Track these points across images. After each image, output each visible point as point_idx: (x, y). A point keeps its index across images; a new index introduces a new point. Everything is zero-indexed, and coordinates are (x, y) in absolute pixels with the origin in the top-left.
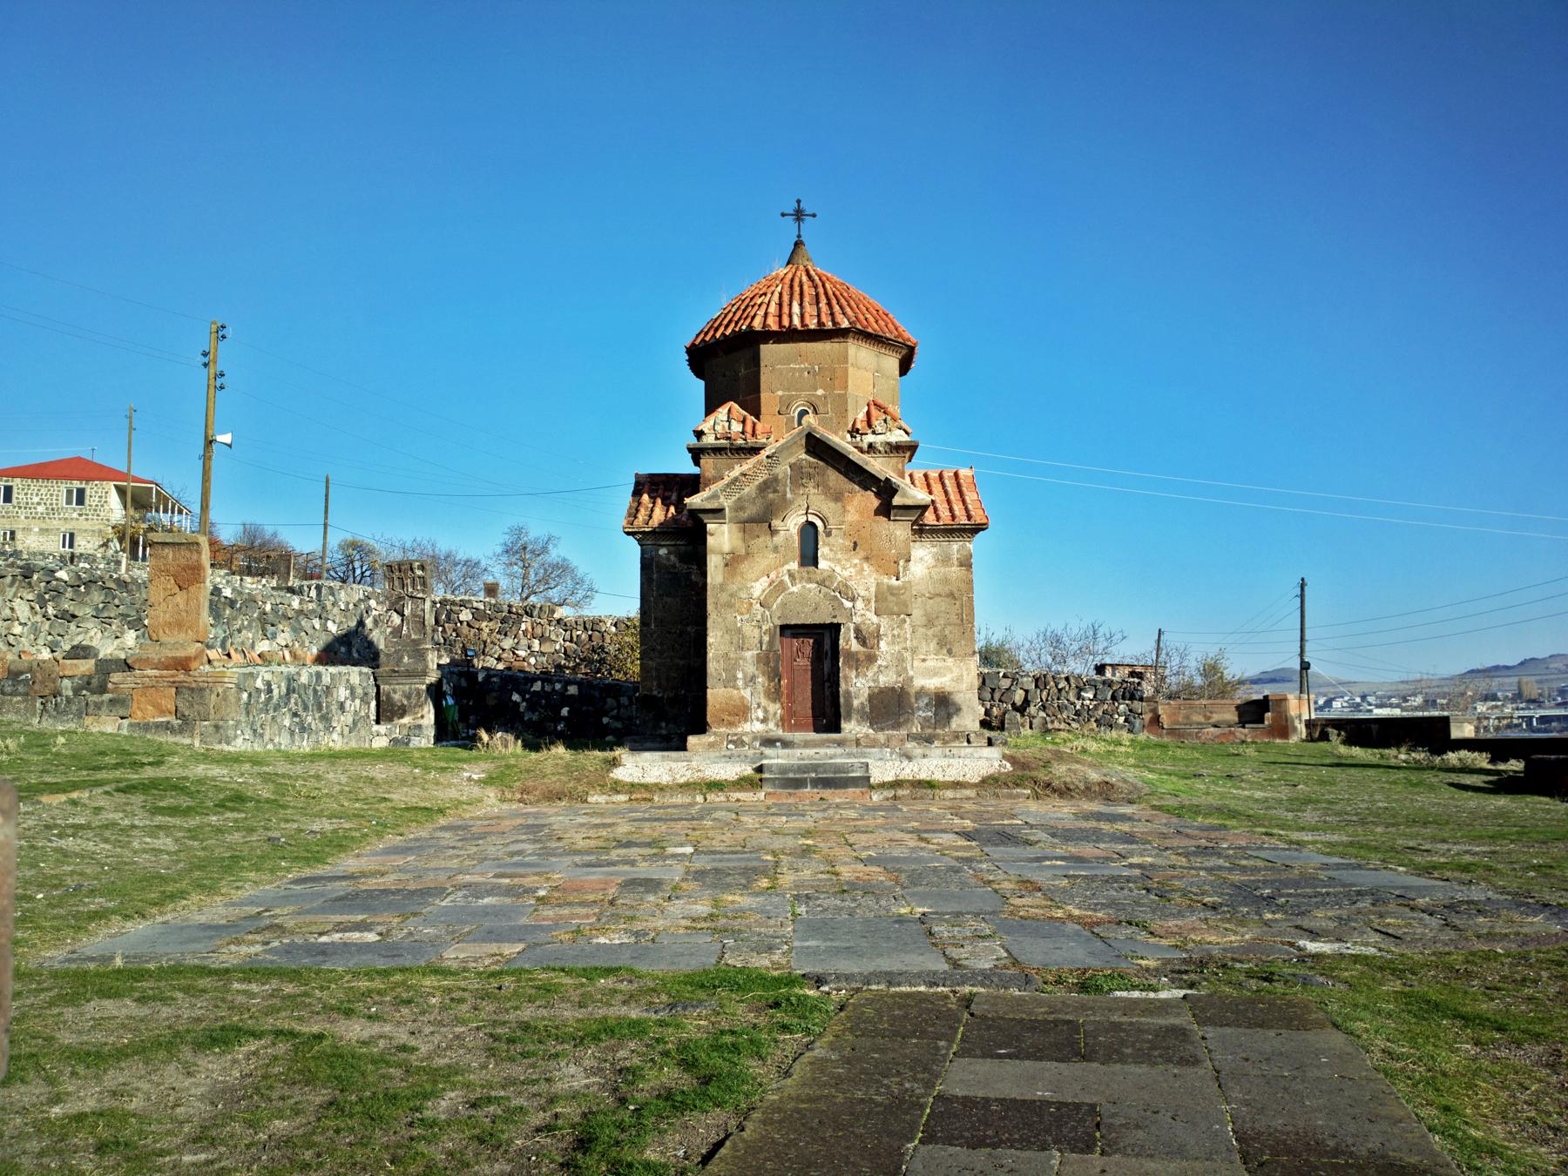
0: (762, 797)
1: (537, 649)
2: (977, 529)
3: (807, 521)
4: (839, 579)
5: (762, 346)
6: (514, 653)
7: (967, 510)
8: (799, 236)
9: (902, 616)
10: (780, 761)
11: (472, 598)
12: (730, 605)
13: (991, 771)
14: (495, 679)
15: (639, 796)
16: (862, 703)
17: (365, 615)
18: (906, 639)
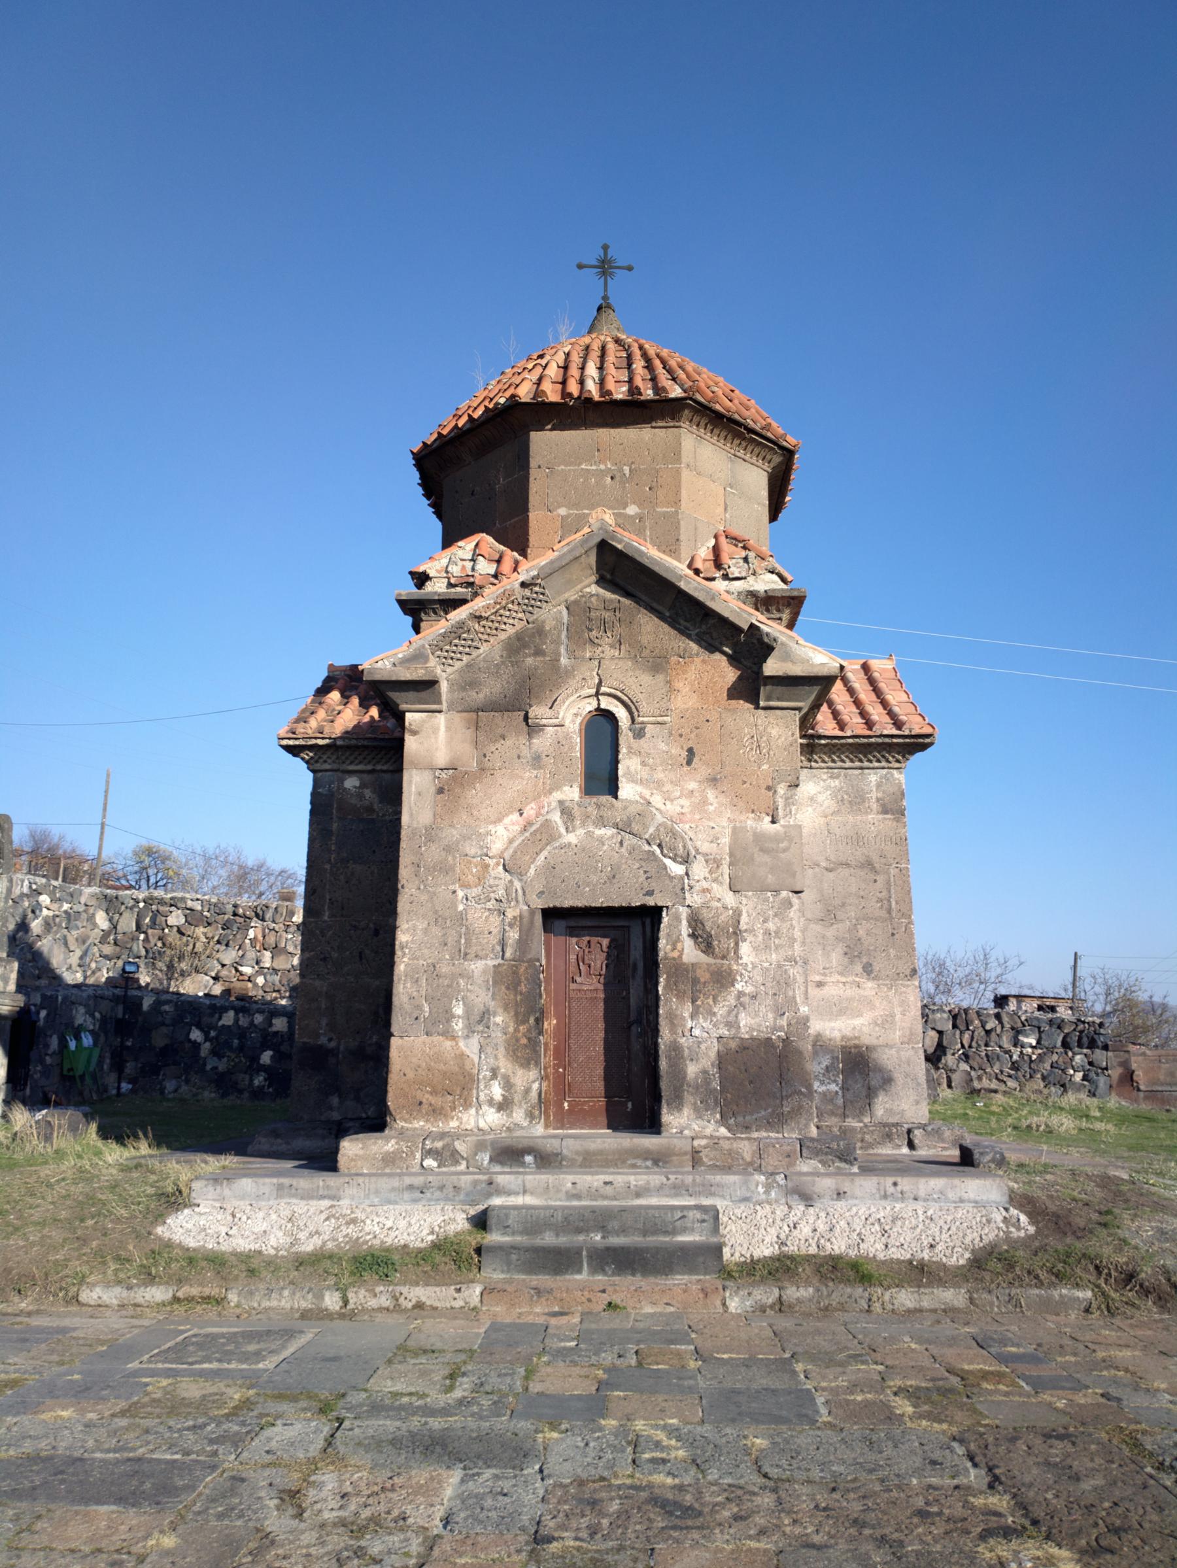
0: (475, 1300)
1: (267, 965)
2: (917, 744)
3: (598, 709)
4: (659, 818)
5: (533, 434)
6: (237, 970)
7: (891, 714)
8: (605, 298)
9: (784, 894)
10: (529, 1200)
11: (187, 896)
12: (445, 869)
13: (990, 1235)
14: (166, 1008)
15: (195, 1291)
16: (705, 1072)
17: (30, 915)
18: (793, 940)
